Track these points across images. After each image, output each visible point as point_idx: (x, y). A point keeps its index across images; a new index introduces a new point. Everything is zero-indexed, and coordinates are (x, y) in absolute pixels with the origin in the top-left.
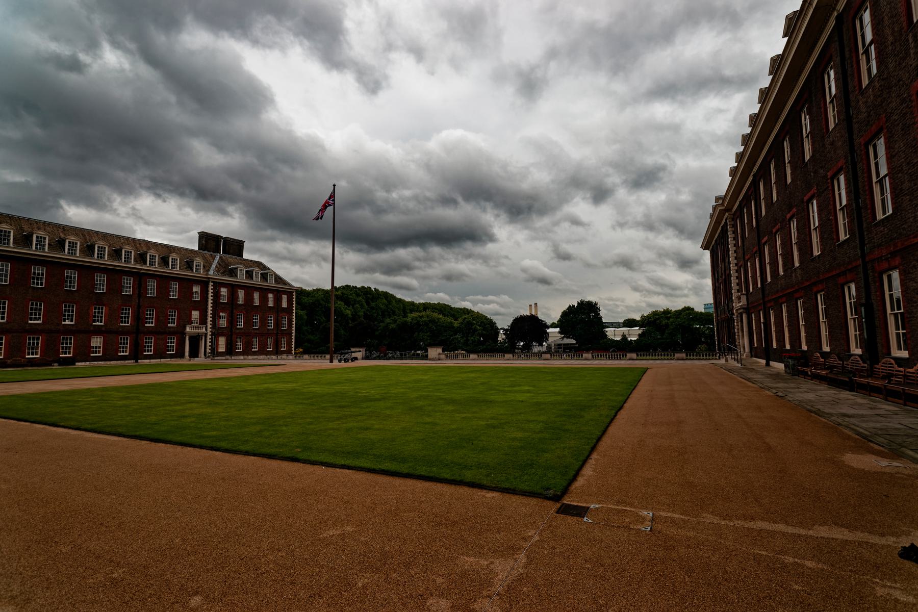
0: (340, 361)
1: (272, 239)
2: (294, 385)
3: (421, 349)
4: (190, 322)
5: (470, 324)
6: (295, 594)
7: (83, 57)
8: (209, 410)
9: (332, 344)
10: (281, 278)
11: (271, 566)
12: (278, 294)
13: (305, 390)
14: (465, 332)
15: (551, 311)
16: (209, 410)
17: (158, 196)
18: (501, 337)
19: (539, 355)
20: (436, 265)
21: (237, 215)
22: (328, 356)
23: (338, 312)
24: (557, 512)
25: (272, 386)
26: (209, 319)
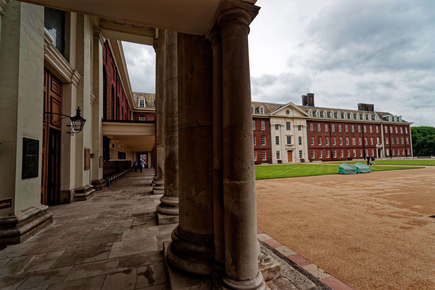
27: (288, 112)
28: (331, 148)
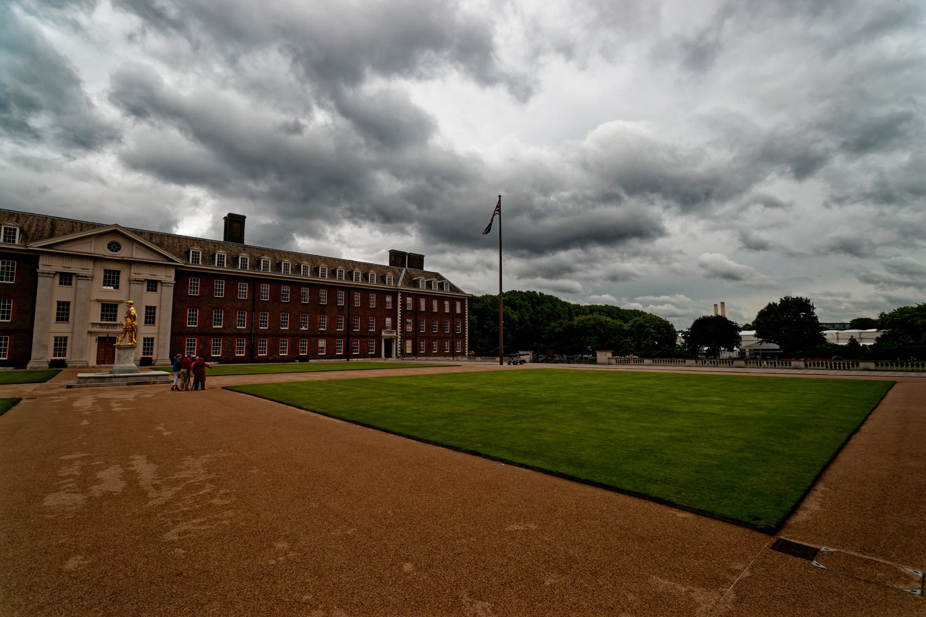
0: (509, 364)
1: (443, 252)
2: (470, 384)
3: (588, 352)
4: (385, 328)
5: (642, 327)
6: (488, 579)
7: (302, 121)
8: (403, 403)
9: (502, 346)
10: (454, 287)
11: (465, 549)
12: (453, 301)
13: (481, 390)
14: (641, 336)
15: (744, 310)
16: (403, 403)
17: (355, 223)
18: (680, 340)
19: (730, 361)
20: (599, 265)
21: (413, 233)
22: (498, 359)
23: (507, 317)
24: (773, 548)
25: (451, 384)
26: (399, 325)
27: (114, 247)
28: (250, 335)
